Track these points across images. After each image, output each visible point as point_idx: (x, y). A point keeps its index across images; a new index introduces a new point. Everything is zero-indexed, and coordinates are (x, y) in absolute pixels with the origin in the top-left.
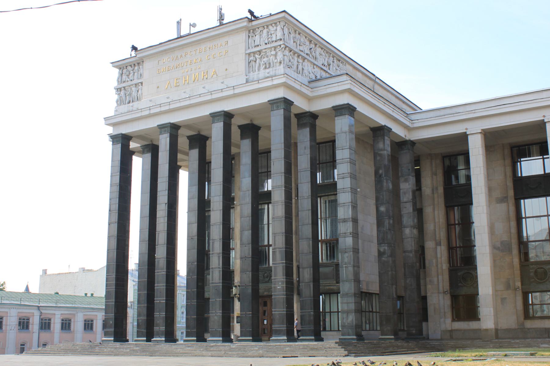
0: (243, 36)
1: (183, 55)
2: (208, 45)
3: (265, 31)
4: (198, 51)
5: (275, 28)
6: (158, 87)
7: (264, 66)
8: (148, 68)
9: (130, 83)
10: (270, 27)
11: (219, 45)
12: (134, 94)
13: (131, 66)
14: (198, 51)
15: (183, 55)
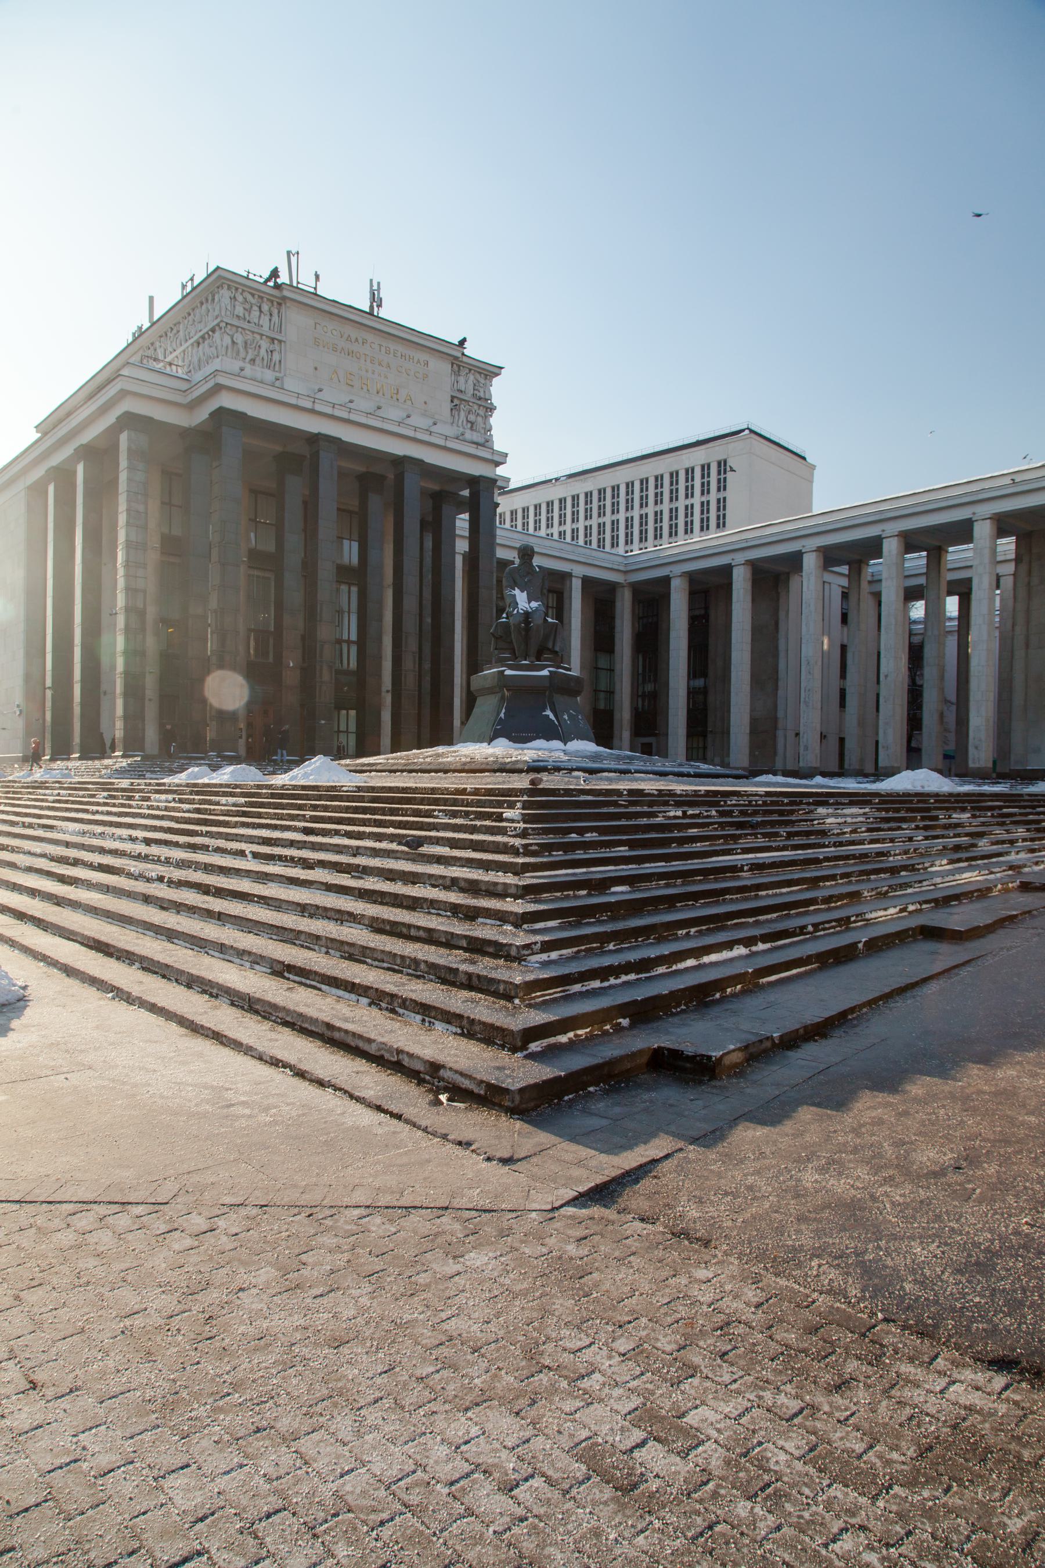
0: (445, 367)
1: (360, 341)
2: (401, 349)
3: (471, 377)
4: (383, 349)
5: (482, 381)
6: (316, 369)
7: (469, 425)
8: (296, 322)
9: (251, 327)
10: (478, 375)
11: (416, 360)
12: (263, 352)
13: (253, 295)
14: (383, 349)
15: (360, 341)
